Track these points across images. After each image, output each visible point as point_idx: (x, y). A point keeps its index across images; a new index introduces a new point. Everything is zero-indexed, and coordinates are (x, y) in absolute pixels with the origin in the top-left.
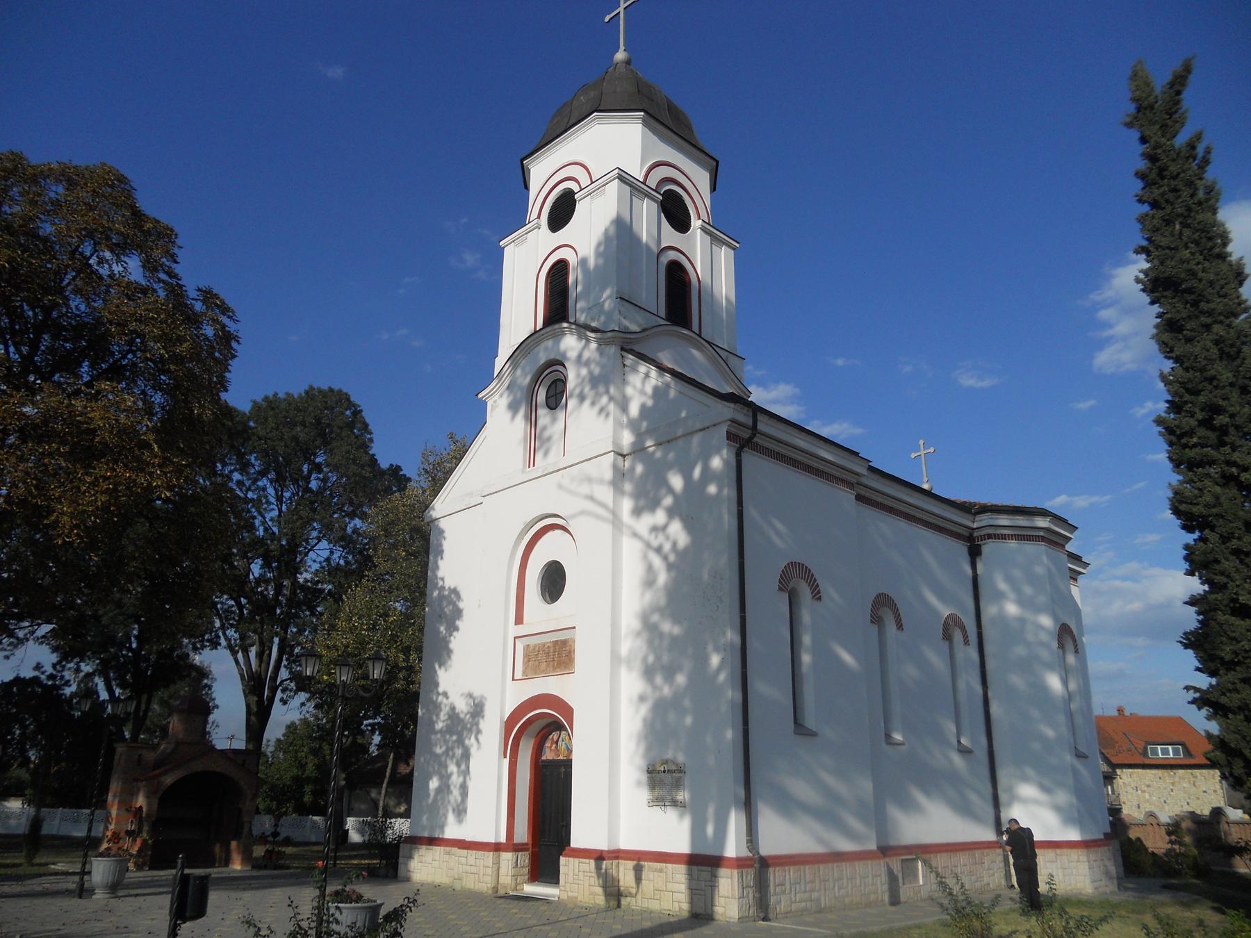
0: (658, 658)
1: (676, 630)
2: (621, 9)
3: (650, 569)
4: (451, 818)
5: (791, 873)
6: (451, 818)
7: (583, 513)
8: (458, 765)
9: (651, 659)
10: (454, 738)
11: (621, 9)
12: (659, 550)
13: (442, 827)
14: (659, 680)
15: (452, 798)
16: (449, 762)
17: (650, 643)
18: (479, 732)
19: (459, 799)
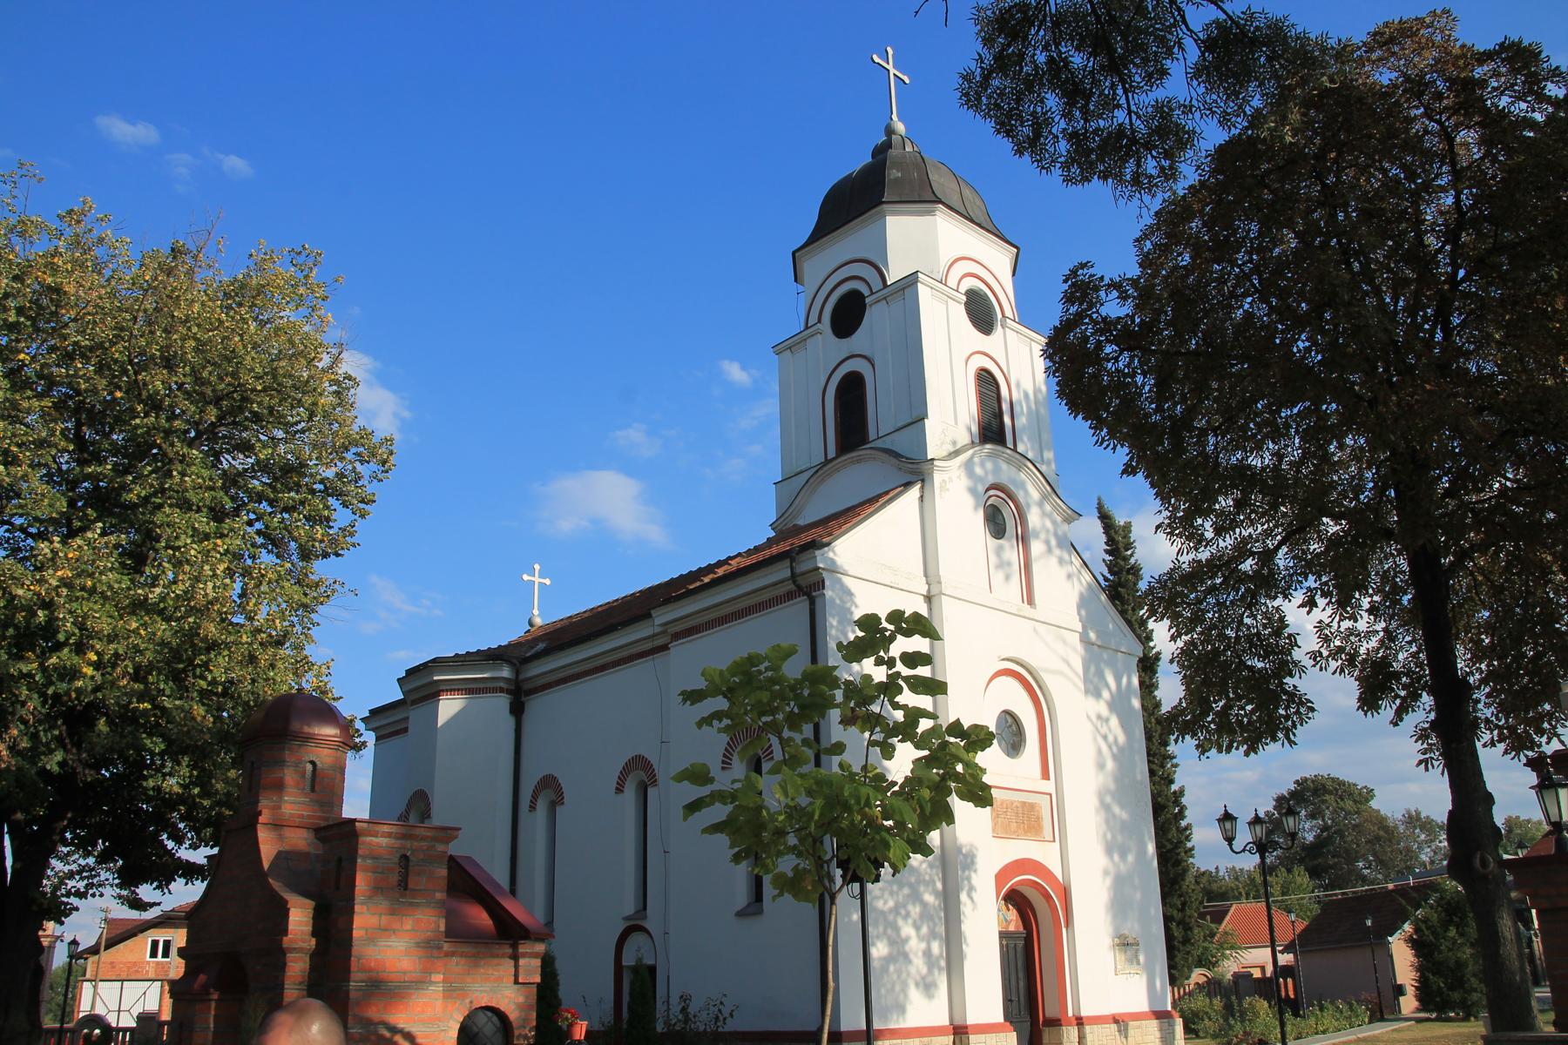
0: (1114, 837)
1: (1124, 815)
2: (890, 67)
3: (1100, 751)
4: (914, 994)
5: (982, 1037)
6: (914, 994)
7: (1061, 673)
8: (918, 928)
9: (1109, 836)
10: (906, 891)
11: (893, 71)
12: (1105, 737)
13: (901, 1009)
14: (1116, 857)
15: (913, 970)
16: (900, 922)
17: (1107, 822)
18: (971, 888)
19: (924, 970)
